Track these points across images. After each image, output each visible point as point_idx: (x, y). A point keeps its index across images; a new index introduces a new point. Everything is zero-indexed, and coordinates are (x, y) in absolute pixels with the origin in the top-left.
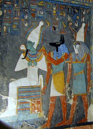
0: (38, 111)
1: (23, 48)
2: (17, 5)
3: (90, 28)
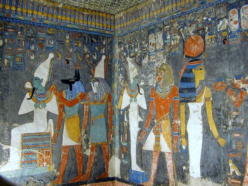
0: (48, 164)
1: (28, 85)
2: (21, 33)
3: (111, 61)
